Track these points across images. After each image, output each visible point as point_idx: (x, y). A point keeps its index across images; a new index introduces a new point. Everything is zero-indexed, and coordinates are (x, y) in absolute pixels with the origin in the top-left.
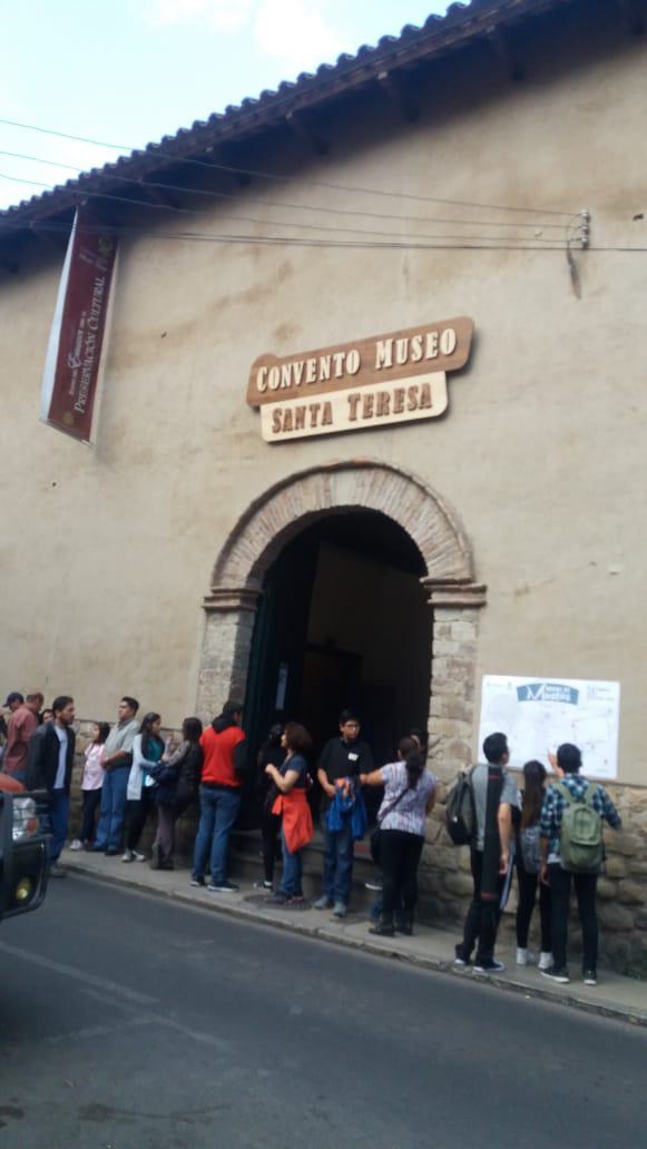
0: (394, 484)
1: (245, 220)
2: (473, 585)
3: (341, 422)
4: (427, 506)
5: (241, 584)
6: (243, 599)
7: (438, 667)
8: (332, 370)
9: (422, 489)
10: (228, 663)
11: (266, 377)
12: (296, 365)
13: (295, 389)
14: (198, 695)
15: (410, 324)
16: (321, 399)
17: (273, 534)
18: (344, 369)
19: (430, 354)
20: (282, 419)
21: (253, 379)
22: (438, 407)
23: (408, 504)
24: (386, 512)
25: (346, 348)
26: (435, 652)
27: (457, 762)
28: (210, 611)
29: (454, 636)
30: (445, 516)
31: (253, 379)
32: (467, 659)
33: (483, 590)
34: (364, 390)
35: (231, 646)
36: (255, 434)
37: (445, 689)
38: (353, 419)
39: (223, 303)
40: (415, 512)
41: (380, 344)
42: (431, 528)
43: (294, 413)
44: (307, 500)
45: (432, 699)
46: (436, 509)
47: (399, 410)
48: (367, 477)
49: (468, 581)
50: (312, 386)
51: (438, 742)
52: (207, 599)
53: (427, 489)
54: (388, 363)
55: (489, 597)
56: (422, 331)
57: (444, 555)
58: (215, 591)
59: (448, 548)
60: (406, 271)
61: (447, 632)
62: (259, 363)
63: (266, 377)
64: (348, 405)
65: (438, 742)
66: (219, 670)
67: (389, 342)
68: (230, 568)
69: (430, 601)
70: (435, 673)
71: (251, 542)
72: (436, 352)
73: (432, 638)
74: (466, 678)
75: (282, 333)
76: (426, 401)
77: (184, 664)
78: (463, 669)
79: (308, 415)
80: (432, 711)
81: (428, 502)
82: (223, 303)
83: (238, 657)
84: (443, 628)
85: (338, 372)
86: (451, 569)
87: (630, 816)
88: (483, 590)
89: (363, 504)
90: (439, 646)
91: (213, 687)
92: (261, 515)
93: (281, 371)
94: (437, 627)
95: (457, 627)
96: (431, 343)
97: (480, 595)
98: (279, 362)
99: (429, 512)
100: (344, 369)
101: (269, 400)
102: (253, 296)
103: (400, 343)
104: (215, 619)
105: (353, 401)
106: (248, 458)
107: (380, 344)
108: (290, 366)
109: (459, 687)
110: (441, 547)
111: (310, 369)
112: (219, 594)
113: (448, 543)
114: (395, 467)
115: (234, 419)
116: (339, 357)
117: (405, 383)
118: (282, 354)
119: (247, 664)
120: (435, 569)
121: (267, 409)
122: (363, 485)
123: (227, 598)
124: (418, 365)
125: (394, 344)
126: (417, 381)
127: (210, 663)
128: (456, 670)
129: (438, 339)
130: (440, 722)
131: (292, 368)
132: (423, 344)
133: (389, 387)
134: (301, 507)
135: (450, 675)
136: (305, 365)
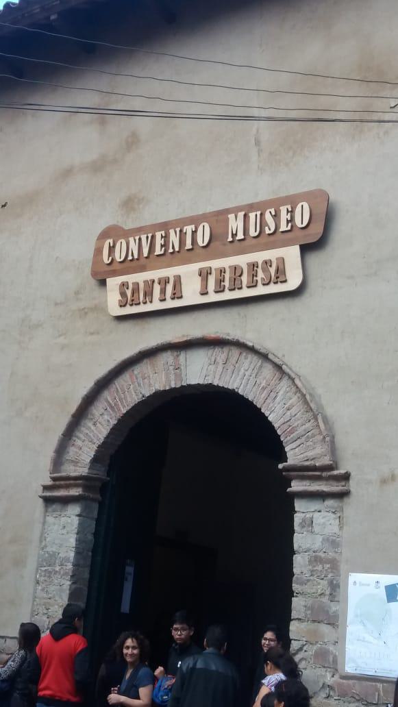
0: (249, 363)
1: (87, 91)
2: (335, 472)
3: (191, 296)
4: (285, 384)
5: (83, 470)
6: (86, 488)
7: (300, 563)
8: (182, 242)
9: (278, 367)
10: (67, 560)
11: (112, 249)
12: (144, 238)
13: (143, 261)
14: (35, 597)
15: (263, 196)
16: (170, 272)
17: (119, 415)
18: (194, 241)
19: (283, 227)
20: (129, 293)
21: (98, 251)
22: (293, 282)
23: (263, 384)
24: (240, 392)
25: (196, 220)
26: (296, 547)
27: (321, 671)
28: (48, 501)
29: (316, 529)
30: (304, 396)
31: (98, 251)
32: (331, 555)
33: (346, 477)
34: (216, 264)
35: (72, 541)
36: (101, 308)
37: (307, 588)
39: (67, 173)
40: (271, 392)
41: (232, 216)
43: (142, 286)
44: (156, 379)
45: (294, 599)
46: (294, 389)
47: (253, 285)
48: (220, 354)
49: (330, 468)
50: (163, 258)
51: (301, 649)
52: (46, 488)
53: (284, 367)
54: (240, 236)
55: (353, 485)
56: (276, 203)
57: (303, 439)
58: (54, 479)
60: (258, 143)
62: (104, 235)
63: (112, 249)
64: (200, 278)
65: (301, 649)
66: (57, 568)
67: (241, 215)
68: (72, 452)
69: (289, 490)
71: (95, 424)
72: (290, 224)
73: (293, 532)
75: (129, 204)
76: (280, 276)
77: (19, 562)
78: (328, 566)
79: (157, 289)
80: (294, 614)
81: (285, 383)
82: (67, 173)
83: (78, 553)
84: (304, 520)
85: (189, 245)
86: (310, 454)
88: (346, 477)
91: (52, 588)
92: (107, 395)
94: (298, 518)
95: (319, 519)
96: (284, 216)
97: (343, 483)
98: (126, 234)
100: (194, 241)
101: (115, 273)
102: (97, 167)
103: (252, 216)
104: (54, 511)
105: (204, 274)
106: (92, 334)
107: (232, 216)
108: (137, 238)
110: (300, 430)
111: (159, 241)
112: (59, 481)
113: (308, 425)
114: (250, 344)
115: (77, 293)
116: (189, 229)
117: (259, 257)
118: (129, 225)
119: (89, 562)
120: (295, 455)
121: (113, 283)
123: (67, 487)
124: (272, 238)
125: (246, 216)
126: (271, 255)
128: (320, 568)
129: (292, 212)
130: (303, 626)
131: (140, 239)
132: (276, 216)
133: (242, 260)
134: (150, 385)
135: (312, 573)
136: (153, 237)
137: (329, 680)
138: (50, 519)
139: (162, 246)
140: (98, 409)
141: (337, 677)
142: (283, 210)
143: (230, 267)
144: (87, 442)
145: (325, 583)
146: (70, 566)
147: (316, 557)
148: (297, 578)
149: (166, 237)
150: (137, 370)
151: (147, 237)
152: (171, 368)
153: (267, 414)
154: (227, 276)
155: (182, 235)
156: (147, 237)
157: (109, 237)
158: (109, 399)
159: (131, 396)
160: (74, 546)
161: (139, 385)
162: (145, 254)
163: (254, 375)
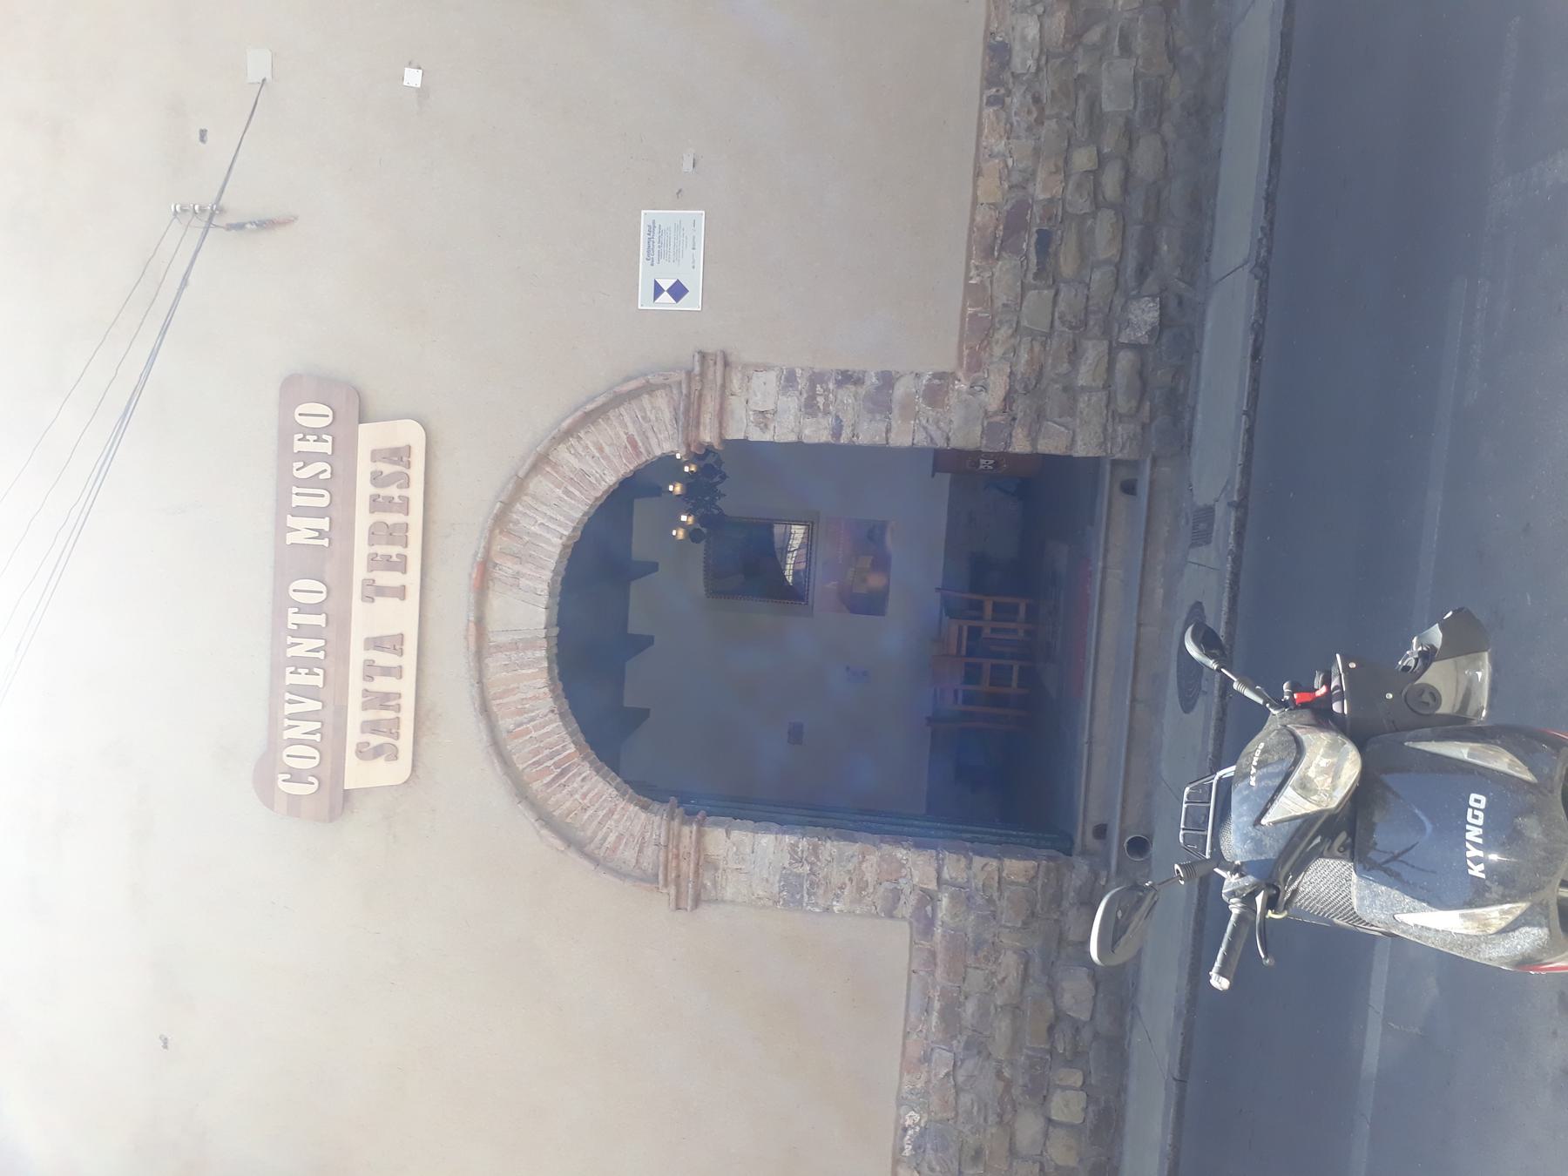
2: (697, 369)
3: (400, 617)
7: (816, 432)
8: (313, 632)
10: (794, 847)
11: (296, 776)
12: (290, 709)
16: (358, 655)
18: (315, 609)
19: (326, 448)
20: (376, 740)
22: (409, 434)
23: (559, 492)
26: (792, 438)
27: (953, 399)
28: (697, 901)
29: (770, 406)
32: (802, 383)
33: (703, 356)
34: (360, 571)
37: (847, 420)
38: (401, 593)
42: (601, 450)
43: (372, 715)
49: (689, 373)
54: (324, 524)
58: (666, 885)
59: (635, 420)
61: (763, 418)
63: (296, 776)
64: (379, 600)
67: (291, 521)
70: (824, 437)
71: (585, 809)
74: (831, 386)
76: (399, 455)
79: (382, 684)
80: (879, 440)
84: (757, 424)
86: (667, 415)
87: (1018, 138)
88: (703, 356)
89: (547, 575)
90: (783, 431)
92: (536, 786)
93: (293, 742)
94: (756, 435)
96: (310, 446)
99: (577, 455)
100: (315, 609)
103: (297, 501)
104: (715, 883)
105: (374, 592)
107: (291, 538)
108: (287, 722)
109: (847, 396)
110: (632, 430)
111: (302, 679)
113: (627, 419)
116: (294, 618)
117: (364, 489)
120: (666, 442)
121: (357, 774)
122: (517, 576)
126: (364, 468)
127: (795, 890)
128: (821, 400)
130: (896, 423)
132: (308, 458)
133: (363, 519)
134: (536, 698)
135: (827, 413)
137: (963, 386)
138: (729, 893)
139: (311, 673)
140: (563, 802)
141: (960, 375)
142: (299, 446)
143: (371, 544)
144: (611, 823)
145: (840, 392)
146: (804, 843)
147: (806, 406)
148: (833, 435)
149: (298, 663)
150: (506, 723)
151: (291, 727)
152: (514, 656)
153: (603, 487)
154: (382, 550)
155: (302, 631)
156: (291, 702)
157: (274, 780)
158: (548, 779)
159: (548, 734)
160: (772, 837)
161: (533, 719)
162: (317, 706)
163: (543, 508)
